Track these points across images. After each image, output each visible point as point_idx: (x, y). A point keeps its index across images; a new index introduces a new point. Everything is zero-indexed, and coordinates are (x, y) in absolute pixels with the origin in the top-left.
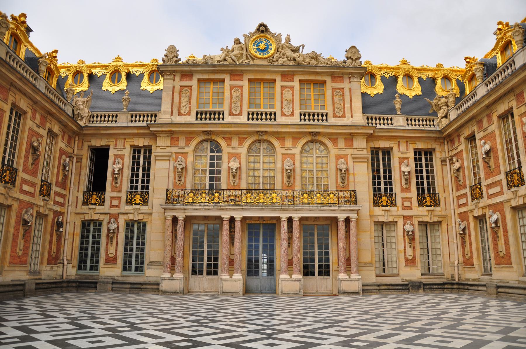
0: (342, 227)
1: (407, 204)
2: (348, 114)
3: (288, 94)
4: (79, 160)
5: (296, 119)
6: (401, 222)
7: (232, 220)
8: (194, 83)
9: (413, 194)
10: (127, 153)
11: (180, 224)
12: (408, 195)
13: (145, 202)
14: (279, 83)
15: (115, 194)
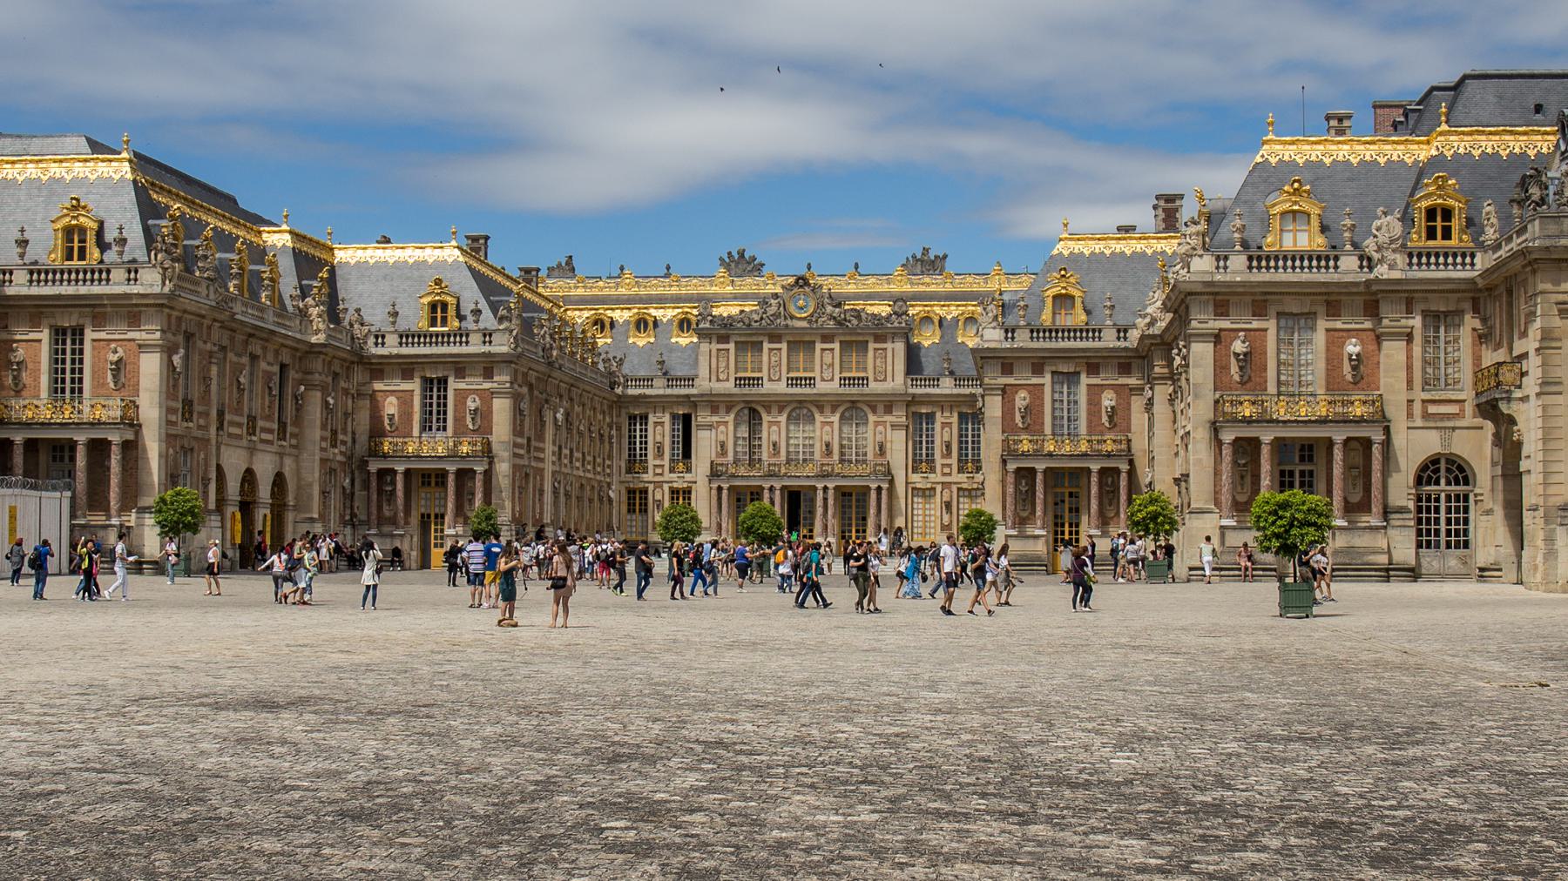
0: (873, 495)
1: (947, 470)
2: (889, 378)
3: (828, 358)
4: (619, 429)
5: (833, 387)
6: (939, 488)
7: (771, 489)
8: (731, 346)
9: (954, 461)
10: (667, 419)
11: (725, 492)
12: (948, 461)
13: (689, 470)
14: (819, 346)
15: (658, 462)
